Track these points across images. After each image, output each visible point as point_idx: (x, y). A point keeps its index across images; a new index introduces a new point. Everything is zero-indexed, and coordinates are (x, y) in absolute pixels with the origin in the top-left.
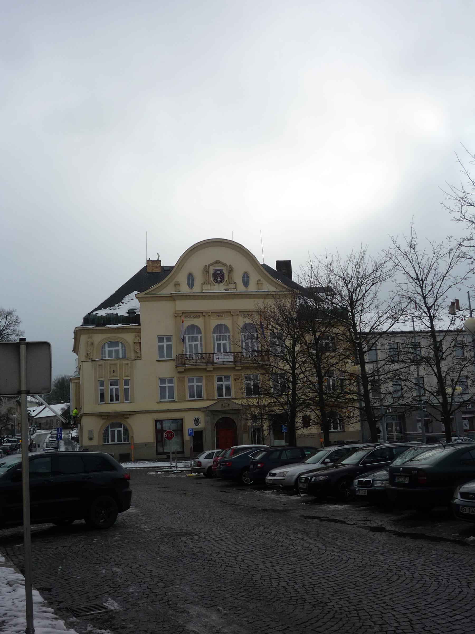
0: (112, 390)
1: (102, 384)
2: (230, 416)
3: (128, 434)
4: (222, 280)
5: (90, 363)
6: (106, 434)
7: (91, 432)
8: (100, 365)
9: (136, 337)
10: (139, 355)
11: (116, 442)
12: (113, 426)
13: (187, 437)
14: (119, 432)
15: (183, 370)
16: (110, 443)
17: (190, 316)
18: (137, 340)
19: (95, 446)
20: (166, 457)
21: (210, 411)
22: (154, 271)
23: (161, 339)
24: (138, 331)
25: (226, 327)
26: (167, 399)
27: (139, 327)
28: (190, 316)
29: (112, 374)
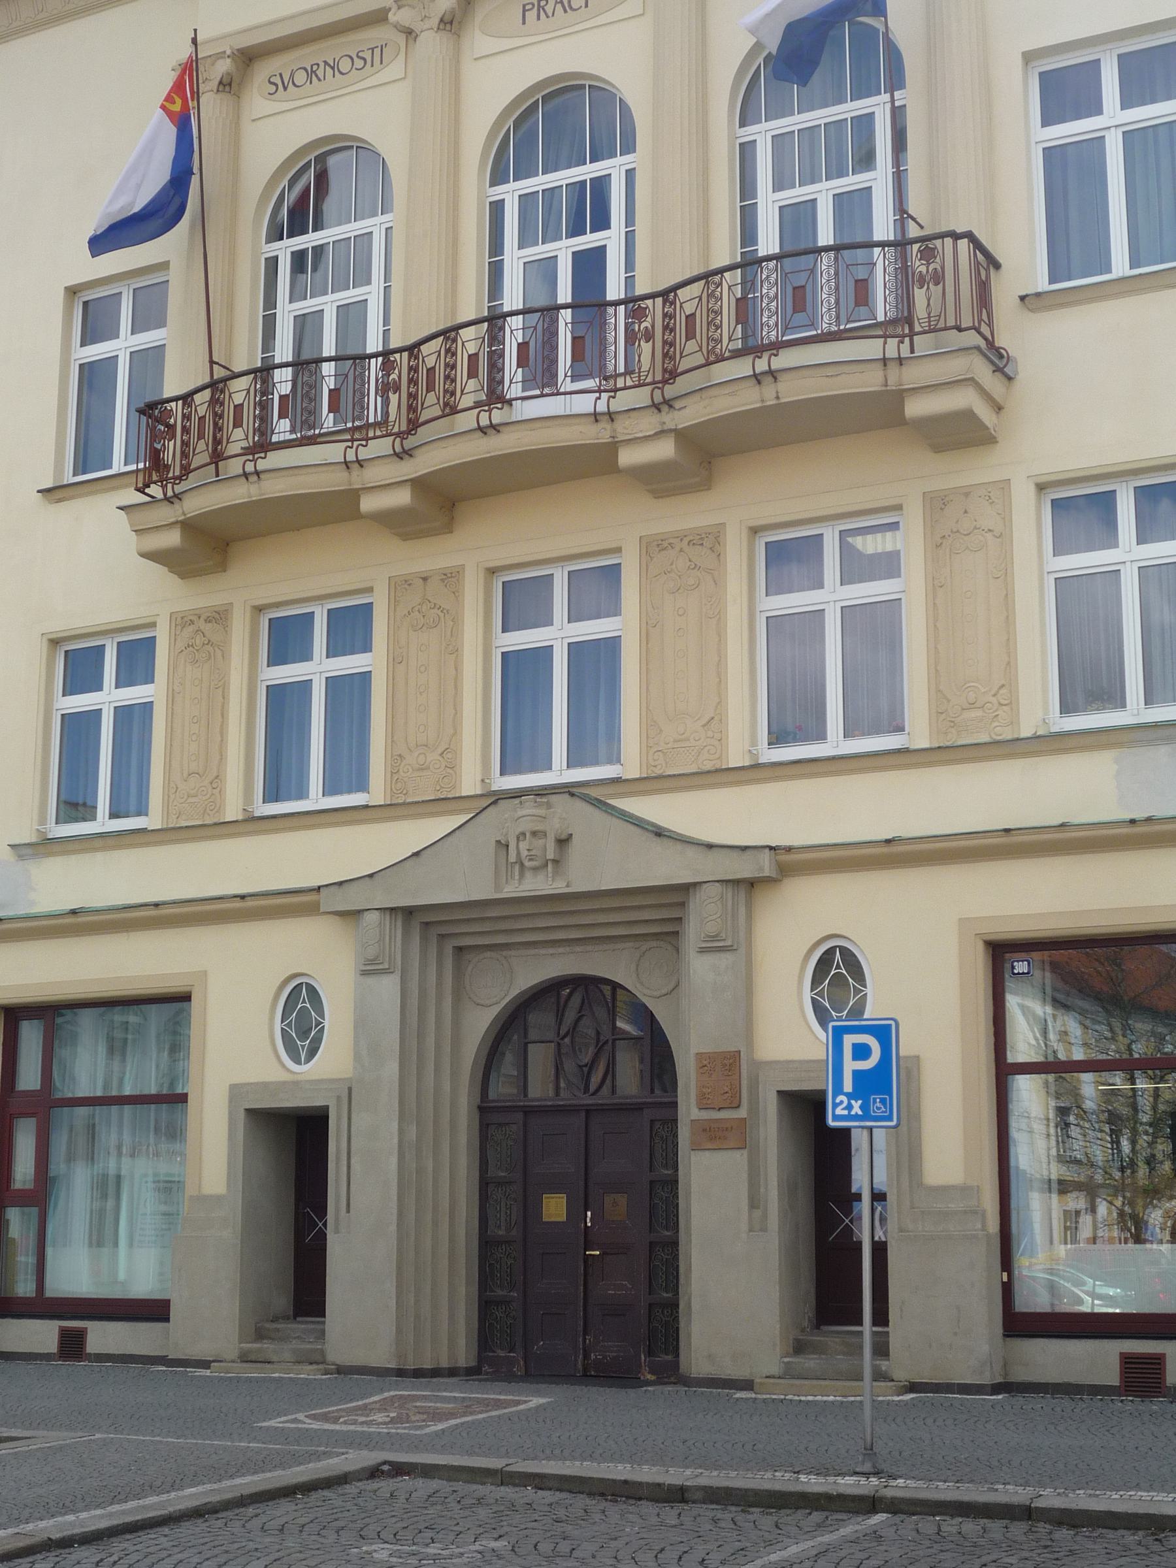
2: (614, 966)
17: (311, 73)
21: (408, 913)
25: (601, 95)
28: (311, 73)
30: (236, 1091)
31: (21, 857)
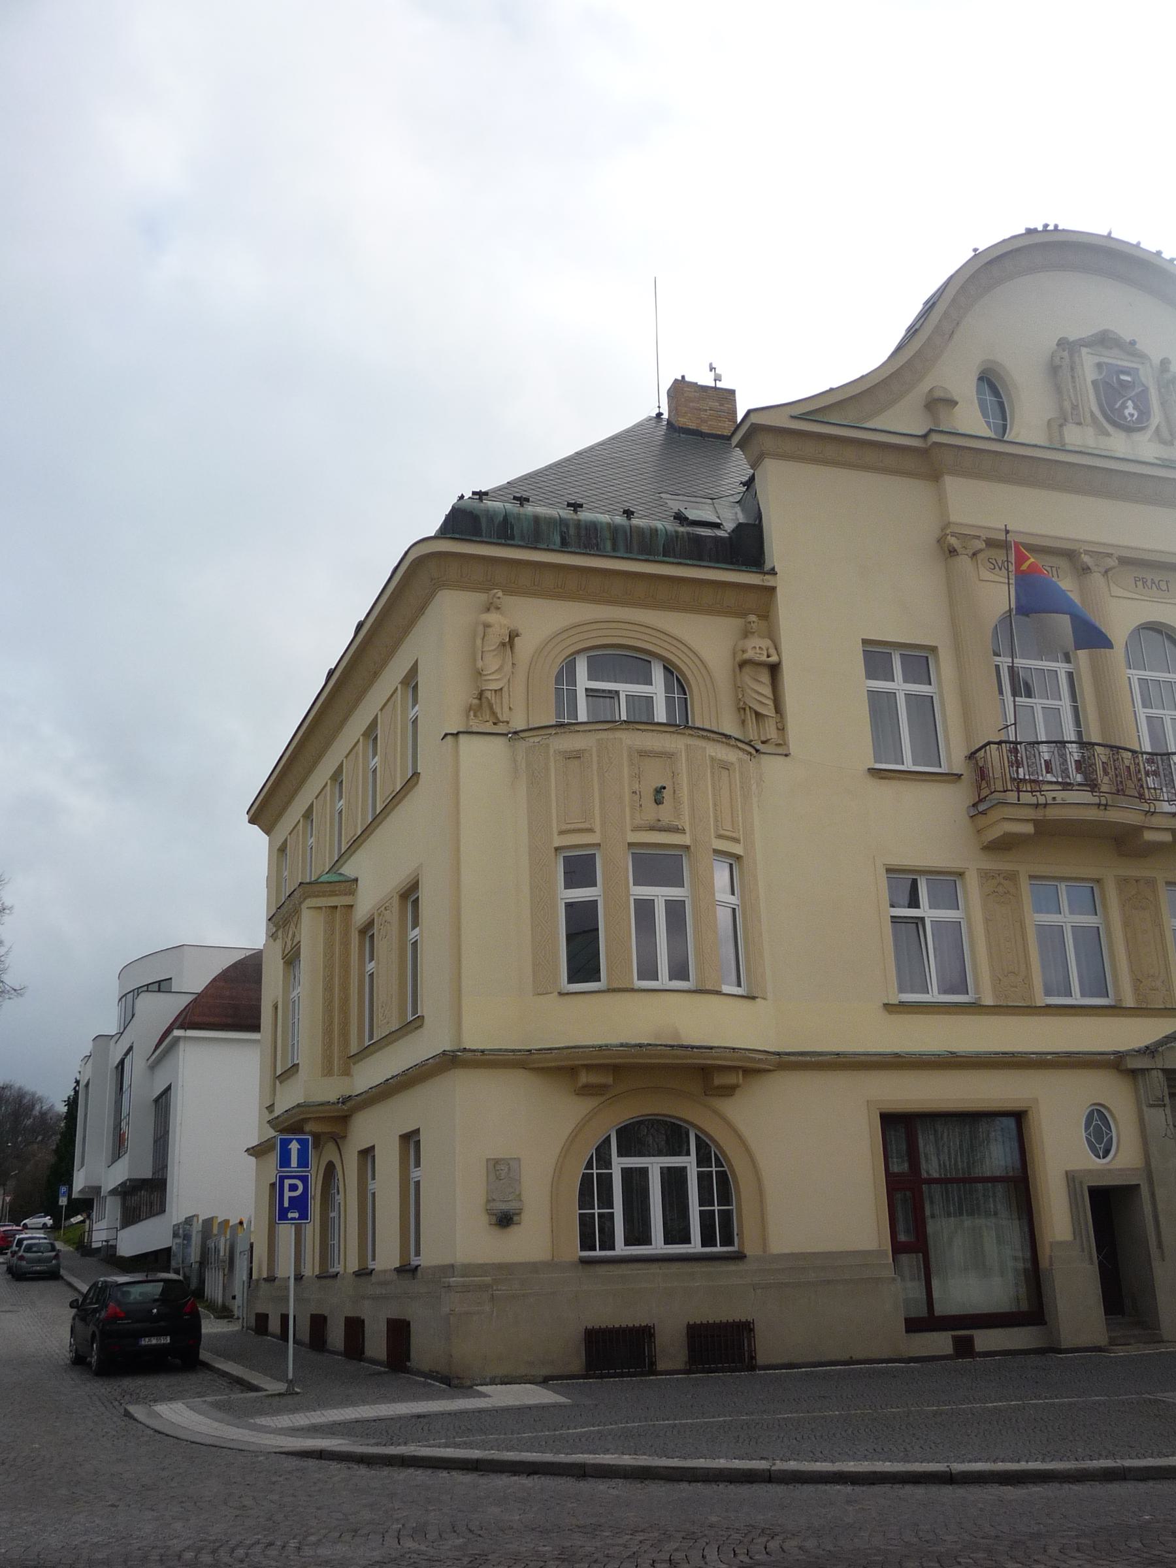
0: (645, 909)
1: (579, 870)
3: (725, 1198)
4: (1144, 413)
5: (499, 744)
6: (593, 1189)
7: (501, 1171)
8: (576, 756)
9: (746, 634)
10: (771, 732)
11: (658, 1245)
12: (632, 1138)
13: (1060, 1219)
14: (674, 1180)
15: (1029, 829)
16: (621, 1248)
18: (757, 648)
19: (534, 1267)
20: (949, 1350)
22: (705, 429)
23: (877, 657)
24: (761, 604)
26: (934, 996)
27: (769, 581)
29: (651, 812)
30: (1071, 1178)
31: (890, 1012)
